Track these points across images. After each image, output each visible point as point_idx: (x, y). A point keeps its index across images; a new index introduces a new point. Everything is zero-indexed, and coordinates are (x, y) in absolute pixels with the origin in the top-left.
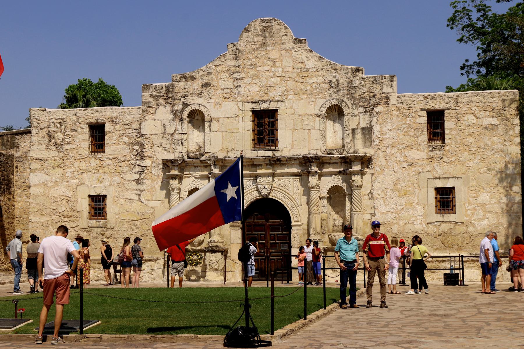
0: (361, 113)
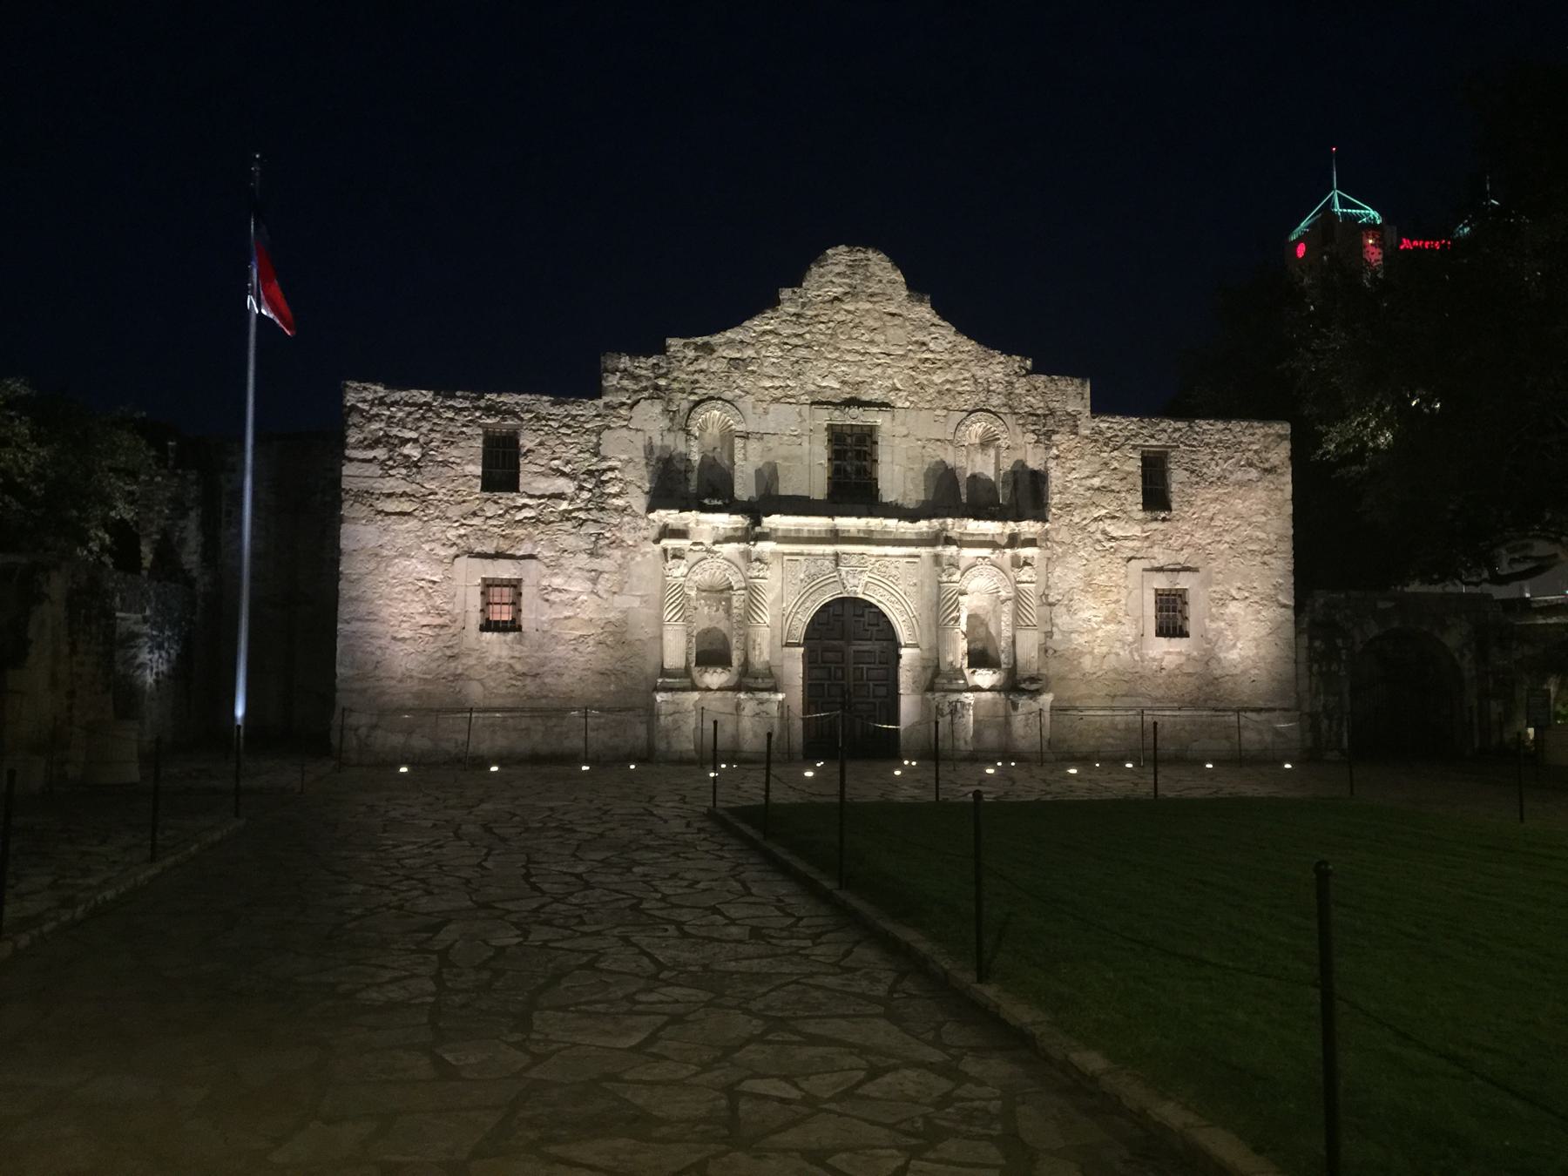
0: (1030, 443)
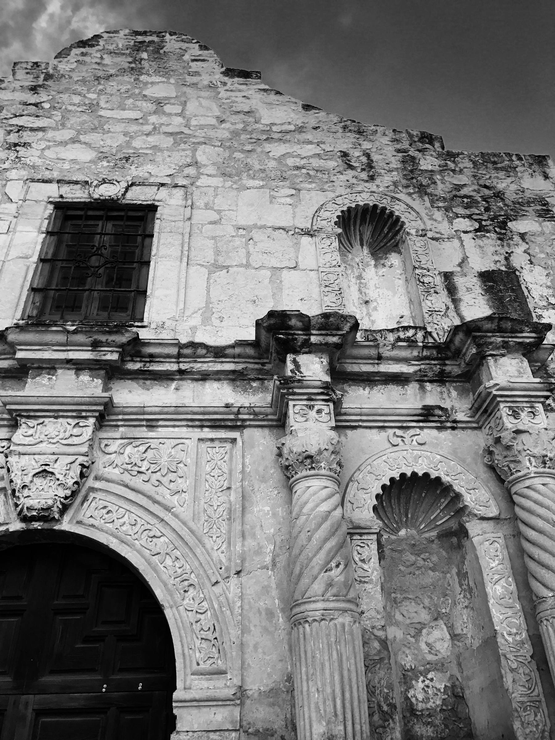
0: (465, 232)
